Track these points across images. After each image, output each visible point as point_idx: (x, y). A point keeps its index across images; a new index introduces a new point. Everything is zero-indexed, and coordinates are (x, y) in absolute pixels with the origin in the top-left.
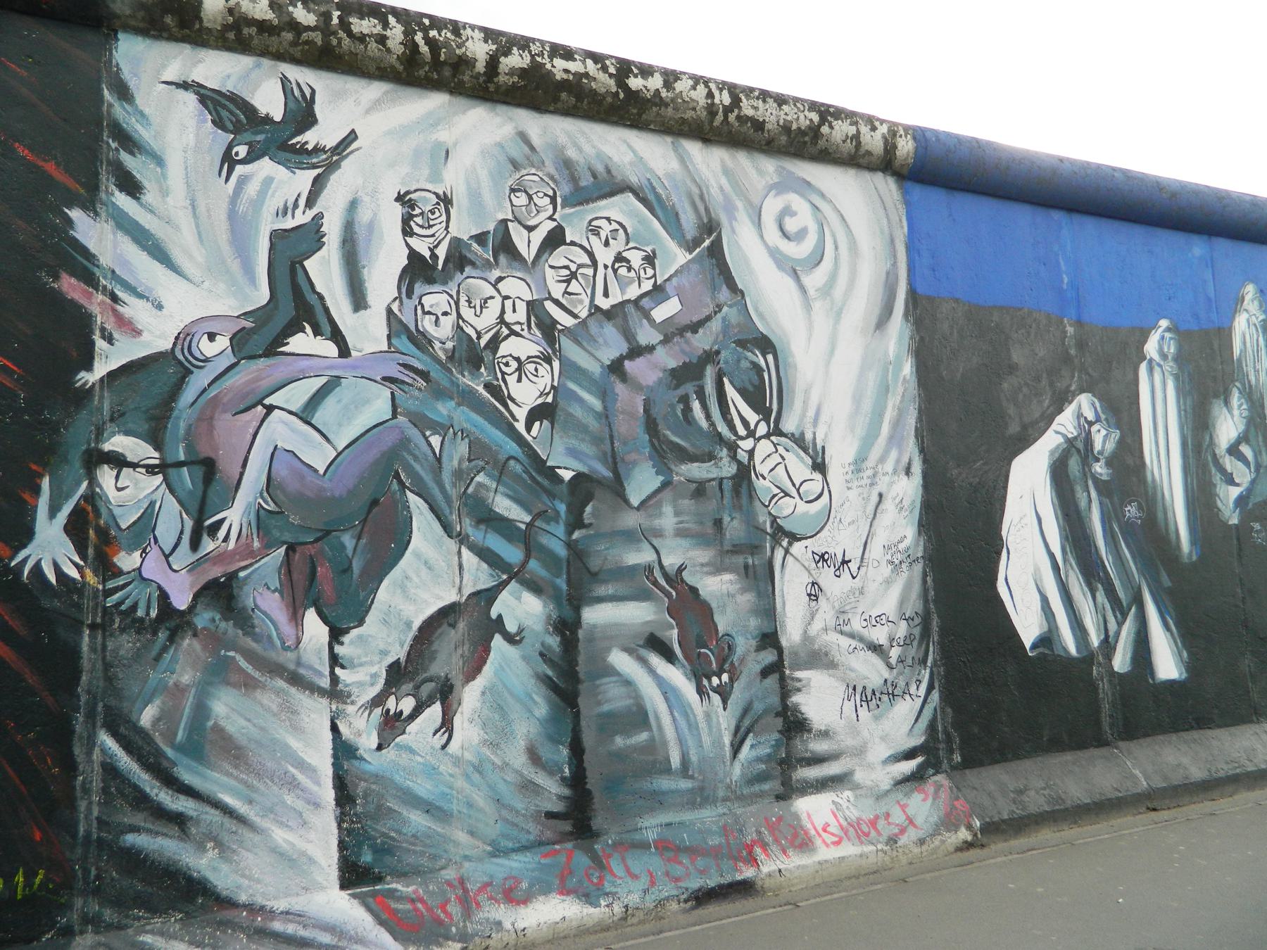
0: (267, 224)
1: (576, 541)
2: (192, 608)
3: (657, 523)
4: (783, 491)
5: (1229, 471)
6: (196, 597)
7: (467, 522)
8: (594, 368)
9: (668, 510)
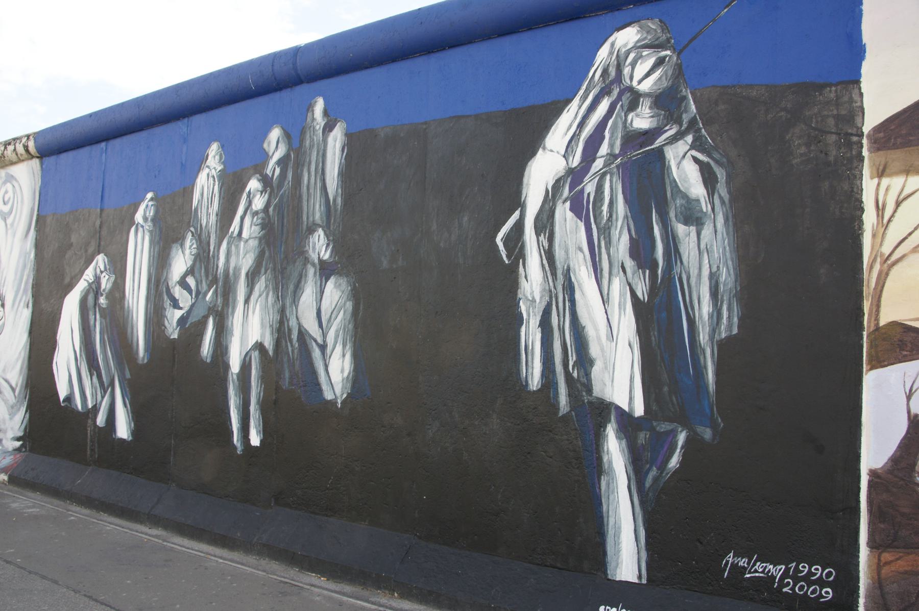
5: (177, 298)
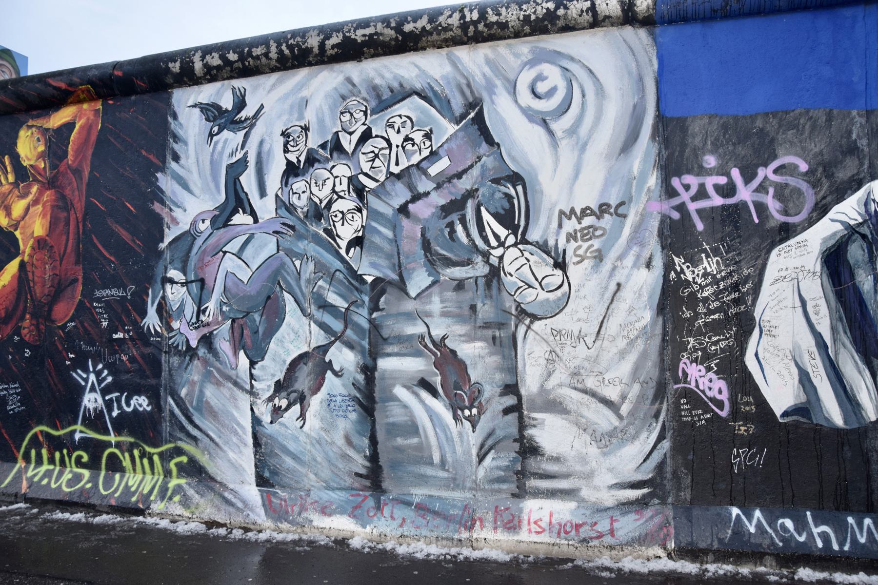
0: (226, 162)
1: (375, 319)
2: (197, 347)
3: (428, 308)
4: (527, 284)
6: (199, 342)
7: (313, 307)
8: (388, 211)
9: (436, 299)
